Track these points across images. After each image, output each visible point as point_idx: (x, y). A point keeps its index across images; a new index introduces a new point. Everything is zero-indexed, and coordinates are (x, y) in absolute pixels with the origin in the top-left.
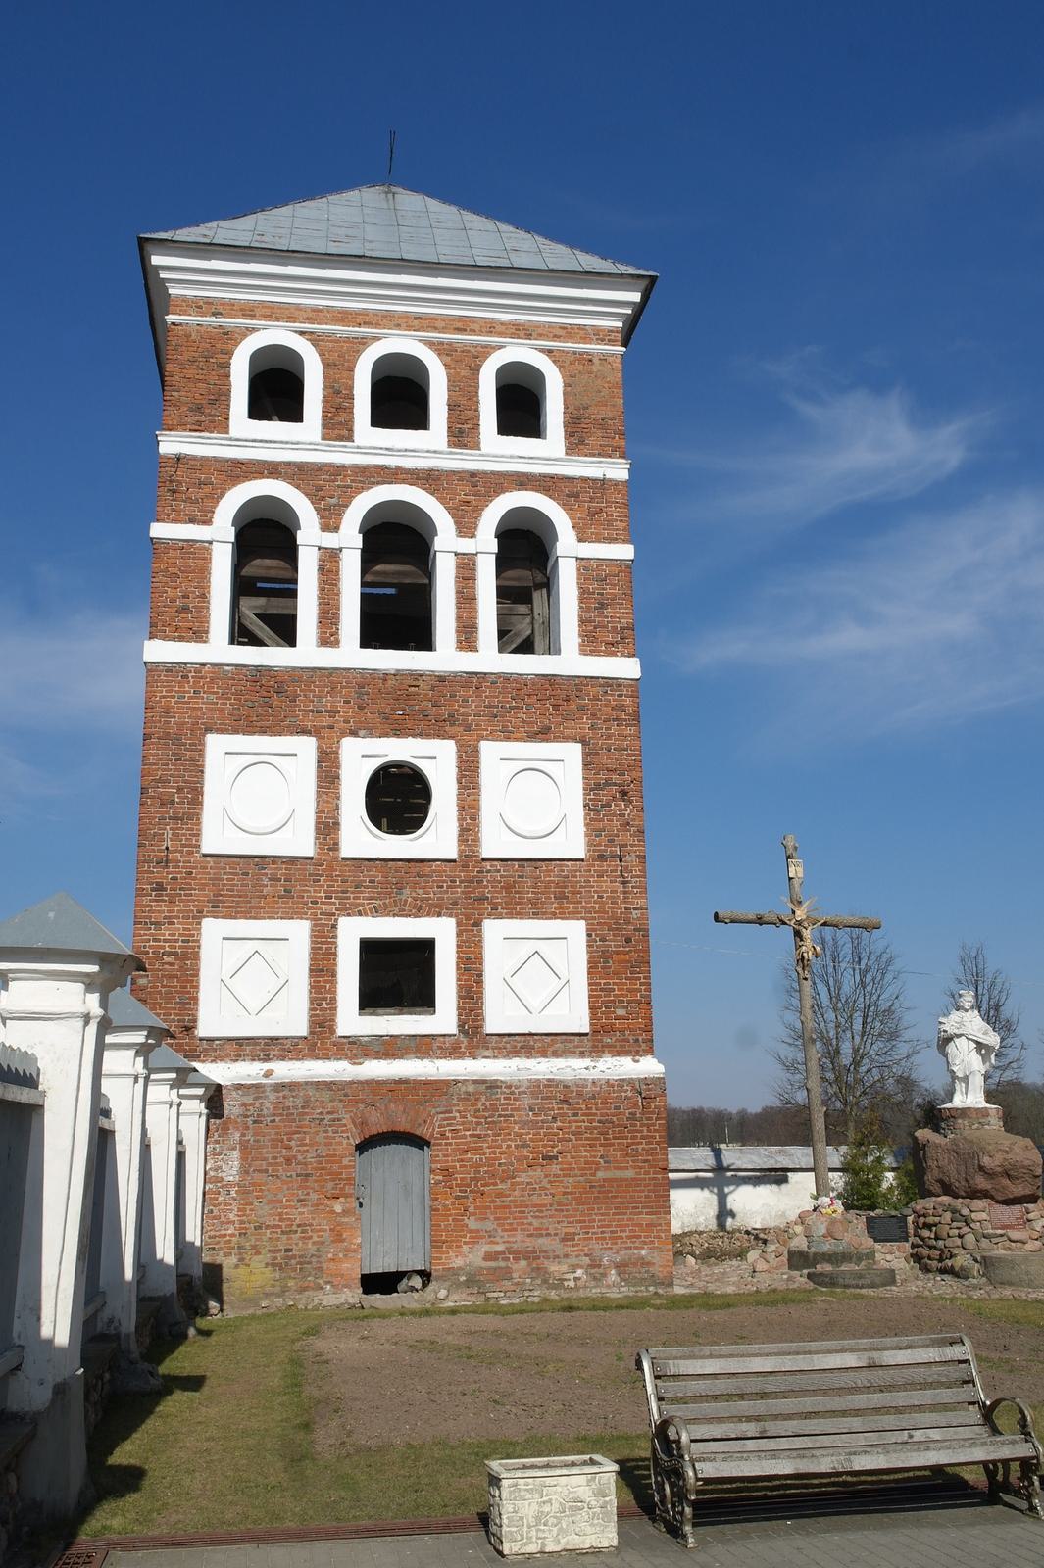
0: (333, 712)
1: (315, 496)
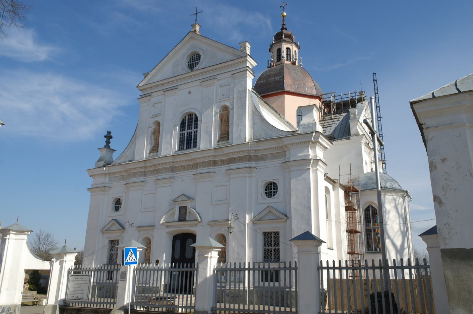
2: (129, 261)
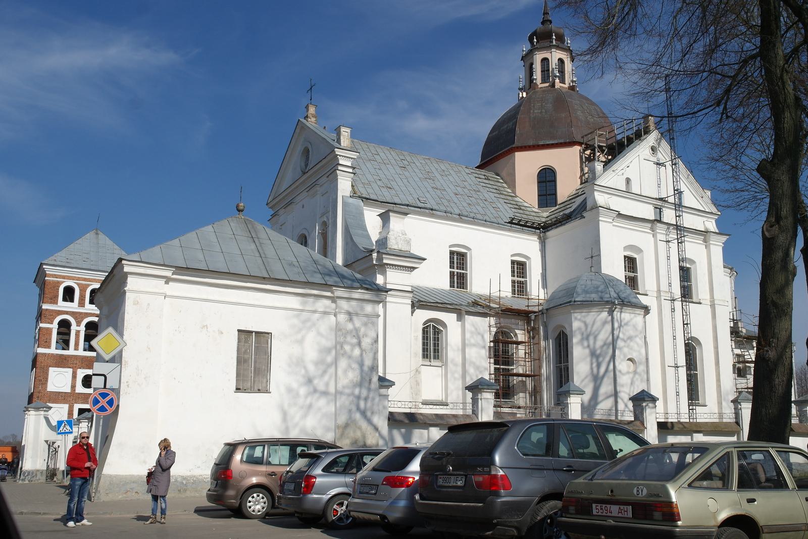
0: (76, 364)
1: (75, 319)
2: (62, 431)
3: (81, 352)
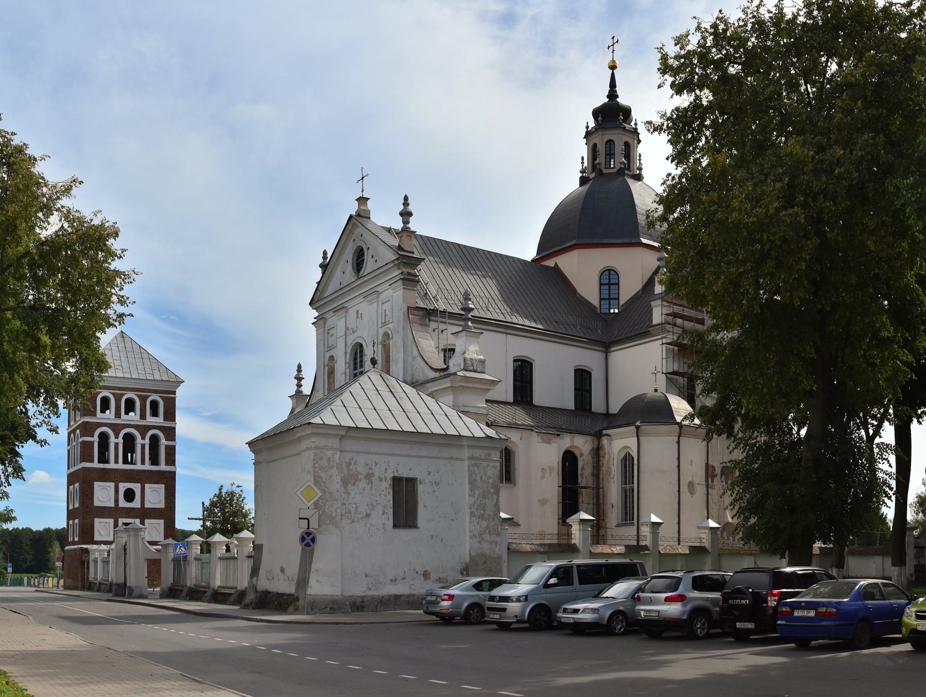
1: (113, 431)
3: (121, 466)
